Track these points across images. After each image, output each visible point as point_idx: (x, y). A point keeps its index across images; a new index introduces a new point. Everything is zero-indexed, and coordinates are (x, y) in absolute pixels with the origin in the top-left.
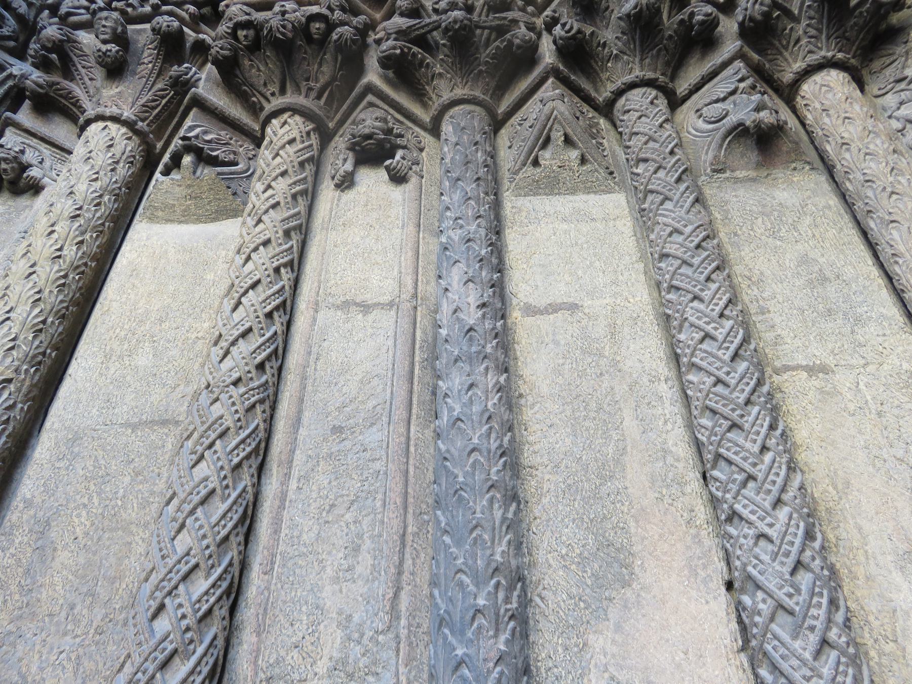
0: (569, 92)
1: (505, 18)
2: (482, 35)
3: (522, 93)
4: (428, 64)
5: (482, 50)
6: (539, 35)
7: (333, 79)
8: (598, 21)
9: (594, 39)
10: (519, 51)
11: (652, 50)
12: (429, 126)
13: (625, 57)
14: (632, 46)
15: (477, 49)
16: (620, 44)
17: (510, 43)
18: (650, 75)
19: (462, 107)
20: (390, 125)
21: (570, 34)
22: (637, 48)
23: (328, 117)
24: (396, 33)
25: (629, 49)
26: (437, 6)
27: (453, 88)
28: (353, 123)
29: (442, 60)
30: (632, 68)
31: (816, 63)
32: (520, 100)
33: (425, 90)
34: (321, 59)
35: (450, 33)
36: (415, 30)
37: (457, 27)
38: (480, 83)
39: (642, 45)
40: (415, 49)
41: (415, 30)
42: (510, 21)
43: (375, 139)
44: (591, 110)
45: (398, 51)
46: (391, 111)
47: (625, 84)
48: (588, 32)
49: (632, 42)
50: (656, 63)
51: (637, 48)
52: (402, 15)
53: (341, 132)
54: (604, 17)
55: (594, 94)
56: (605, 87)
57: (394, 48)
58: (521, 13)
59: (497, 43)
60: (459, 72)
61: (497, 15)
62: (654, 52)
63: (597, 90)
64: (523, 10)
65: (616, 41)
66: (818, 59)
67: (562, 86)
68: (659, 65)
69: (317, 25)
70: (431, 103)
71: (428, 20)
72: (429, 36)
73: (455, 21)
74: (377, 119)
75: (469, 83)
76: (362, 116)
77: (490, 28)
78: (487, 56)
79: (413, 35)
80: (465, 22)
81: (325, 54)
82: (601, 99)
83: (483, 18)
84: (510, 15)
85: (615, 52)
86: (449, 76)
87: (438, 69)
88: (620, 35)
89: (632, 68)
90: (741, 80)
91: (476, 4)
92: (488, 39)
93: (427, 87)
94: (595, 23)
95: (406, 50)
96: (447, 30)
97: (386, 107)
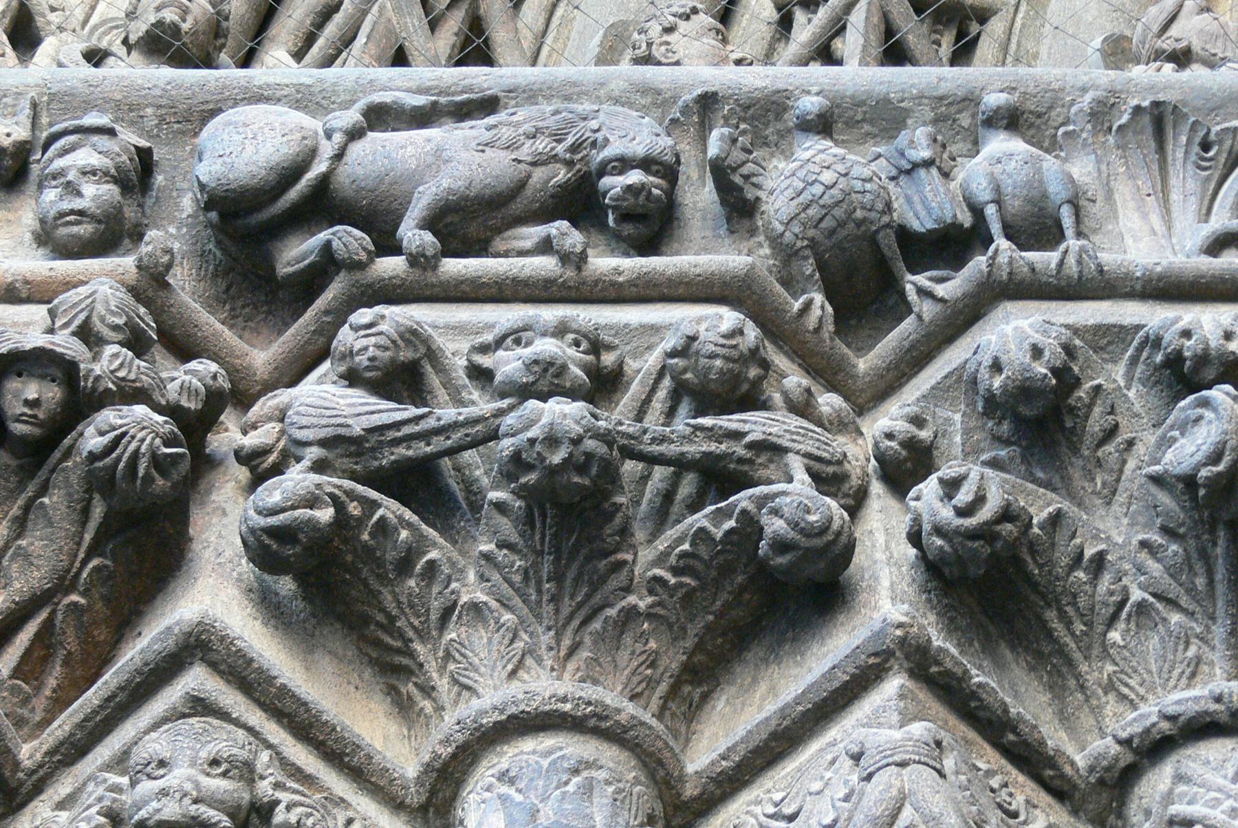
0: (964, 729)
1: (737, 435)
2: (645, 478)
3: (783, 712)
4: (432, 563)
5: (640, 535)
6: (856, 504)
7: (64, 583)
8: (1076, 474)
9: (1061, 537)
10: (782, 560)
12: (415, 797)
13: (1175, 618)
14: (1200, 582)
15: (625, 531)
16: (1155, 567)
17: (750, 527)
19: (548, 741)
20: (264, 788)
22: (1221, 588)
23: (19, 722)
24: (323, 443)
25: (1191, 590)
26: (485, 361)
27: (520, 664)
28: (120, 762)
29: (487, 557)
30: (1198, 660)
32: (774, 736)
33: (411, 654)
34: (27, 509)
35: (531, 478)
36: (396, 442)
37: (557, 458)
38: (623, 656)
40: (390, 508)
41: (396, 442)
42: (752, 446)
44: (1044, 798)
45: (325, 515)
46: (275, 733)
47: (1172, 718)
48: (1039, 515)
49: (1199, 567)
51: (1221, 588)
52: (352, 378)
53: (63, 787)
54: (1099, 463)
55: (1055, 737)
56: (1097, 711)
57: (312, 502)
58: (795, 422)
59: (699, 519)
60: (548, 609)
61: (707, 421)
63: (1065, 718)
64: (803, 408)
65: (1143, 556)
67: (936, 708)
69: (32, 390)
70: (427, 705)
71: (448, 414)
72: (446, 463)
73: (552, 440)
74: (215, 762)
75: (585, 654)
76: (156, 745)
77: (681, 464)
78: (661, 560)
79: (388, 458)
80: (590, 444)
81: (43, 490)
82: (1081, 760)
83: (653, 421)
84: (754, 424)
85: (1136, 595)
86: (507, 617)
87: (471, 590)
88: (1157, 538)
89: (1198, 660)
91: (631, 365)
92: (668, 497)
93: (418, 647)
94: (1067, 480)
95: (354, 509)
96: (518, 463)
97: (256, 717)
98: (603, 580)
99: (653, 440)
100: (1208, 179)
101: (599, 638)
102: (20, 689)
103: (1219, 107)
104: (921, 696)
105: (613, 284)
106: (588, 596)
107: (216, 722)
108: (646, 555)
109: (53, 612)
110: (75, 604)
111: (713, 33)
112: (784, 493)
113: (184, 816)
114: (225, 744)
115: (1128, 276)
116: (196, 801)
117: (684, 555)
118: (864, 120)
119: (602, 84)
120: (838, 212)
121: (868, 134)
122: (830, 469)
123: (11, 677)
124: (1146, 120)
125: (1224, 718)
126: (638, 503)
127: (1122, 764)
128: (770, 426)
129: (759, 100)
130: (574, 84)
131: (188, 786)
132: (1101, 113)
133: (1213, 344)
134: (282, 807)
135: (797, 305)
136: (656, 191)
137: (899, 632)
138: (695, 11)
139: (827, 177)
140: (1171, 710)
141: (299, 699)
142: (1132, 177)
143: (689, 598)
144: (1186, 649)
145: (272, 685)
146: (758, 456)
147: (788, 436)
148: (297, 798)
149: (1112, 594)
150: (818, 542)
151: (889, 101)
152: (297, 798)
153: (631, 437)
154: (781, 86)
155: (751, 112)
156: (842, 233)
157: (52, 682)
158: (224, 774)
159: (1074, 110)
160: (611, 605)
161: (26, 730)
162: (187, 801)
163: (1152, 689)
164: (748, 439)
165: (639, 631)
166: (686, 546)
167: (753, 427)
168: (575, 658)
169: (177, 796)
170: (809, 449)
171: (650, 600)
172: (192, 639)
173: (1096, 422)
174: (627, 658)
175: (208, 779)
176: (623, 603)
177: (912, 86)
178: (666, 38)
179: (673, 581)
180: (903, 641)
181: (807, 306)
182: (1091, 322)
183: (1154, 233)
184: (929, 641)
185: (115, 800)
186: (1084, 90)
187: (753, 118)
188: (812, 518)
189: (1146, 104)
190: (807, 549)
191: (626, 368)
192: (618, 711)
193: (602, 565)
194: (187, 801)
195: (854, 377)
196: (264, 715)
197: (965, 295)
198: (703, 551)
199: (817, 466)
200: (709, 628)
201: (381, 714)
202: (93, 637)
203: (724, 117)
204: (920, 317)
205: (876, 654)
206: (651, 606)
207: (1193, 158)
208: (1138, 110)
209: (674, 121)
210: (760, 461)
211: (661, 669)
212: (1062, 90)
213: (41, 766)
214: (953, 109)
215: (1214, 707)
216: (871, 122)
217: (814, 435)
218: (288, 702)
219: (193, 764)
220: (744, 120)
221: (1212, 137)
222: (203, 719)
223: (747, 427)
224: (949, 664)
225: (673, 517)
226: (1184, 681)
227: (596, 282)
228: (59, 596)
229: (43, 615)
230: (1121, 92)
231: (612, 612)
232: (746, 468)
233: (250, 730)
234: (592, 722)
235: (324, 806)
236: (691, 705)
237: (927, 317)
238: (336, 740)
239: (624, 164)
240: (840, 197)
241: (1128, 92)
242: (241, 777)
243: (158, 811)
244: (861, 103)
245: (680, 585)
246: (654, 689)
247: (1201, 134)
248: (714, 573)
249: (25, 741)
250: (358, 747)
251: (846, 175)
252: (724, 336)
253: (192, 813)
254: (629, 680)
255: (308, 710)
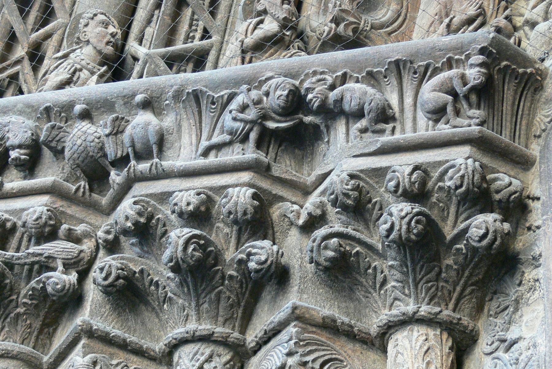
1: (41, 255)
11: (210, 292)
13: (181, 301)
14: (186, 289)
17: (44, 289)
18: (205, 327)
21: (106, 283)
22: (192, 291)
25: (183, 292)
30: (188, 315)
31: (396, 319)
38: (19, 327)
39: (196, 290)
42: (46, 257)
47: (175, 339)
50: (218, 308)
51: (192, 291)
55: (146, 344)
62: (213, 296)
66: (397, 316)
68: (221, 310)
75: (7, 329)
78: (25, 296)
89: (188, 315)
90: (290, 354)
98: (8, 306)
99: (16, 259)
100: (214, 116)
101: (10, 323)
103: (219, 86)
104: (92, 344)
105: (13, 193)
106: (4, 312)
108: (23, 292)
111: (101, 25)
112: (51, 277)
115: (173, 171)
117: (30, 295)
118: (101, 107)
119: (15, 106)
120: (83, 155)
121: (103, 112)
122: (72, 261)
124: (192, 96)
125: (190, 338)
126: (22, 273)
127: (166, 351)
128: (51, 250)
129: (65, 105)
130: (6, 107)
132: (177, 96)
133: (183, 208)
135: (74, 188)
136: (23, 157)
137: (80, 328)
138: (95, 15)
139: (79, 142)
140: (175, 336)
142: (189, 119)
143: (36, 306)
144: (184, 311)
146: (49, 260)
147: (56, 253)
149: (162, 294)
150: (61, 294)
151: (107, 100)
153: (9, 259)
154: (72, 99)
155: (64, 109)
156: (86, 161)
159: (168, 96)
160: (12, 313)
163: (176, 324)
164: (44, 256)
165: (22, 319)
166: (31, 292)
167: (46, 251)
168: (3, 331)
170: (64, 257)
171: (24, 309)
173: (160, 230)
174: (21, 327)
176: (15, 312)
177: (115, 93)
178: (85, 29)
179: (30, 302)
180: (82, 330)
181: (78, 189)
182: (160, 191)
183: (191, 144)
184: (91, 327)
186: (172, 86)
187: (65, 111)
188: (59, 286)
189: (190, 91)
190: (59, 296)
191: (17, 224)
192: (13, 351)
193: (6, 301)
195: (102, 206)
197: (123, 183)
198: (36, 293)
199: (67, 261)
200: (47, 313)
203: (54, 114)
204: (114, 189)
205: (77, 333)
206: (26, 310)
207: (209, 109)
208: (188, 93)
209: (38, 118)
210: (50, 261)
211: (34, 328)
212: (164, 87)
214: (130, 99)
215: (186, 335)
216: (103, 107)
217: (67, 250)
220: (63, 112)
221: (215, 100)
223: (44, 251)
224: (100, 333)
225: (33, 276)
226: (184, 322)
227: (7, 193)
230: (185, 85)
231: (12, 315)
232: (46, 264)
234: (6, 355)
236: (49, 334)
237: (115, 188)
239: (14, 148)
240: (83, 150)
241: (187, 85)
244: (99, 102)
245: (32, 304)
246: (32, 334)
247: (211, 99)
248: (42, 298)
251: (85, 140)
252: (34, 221)
254: (22, 335)
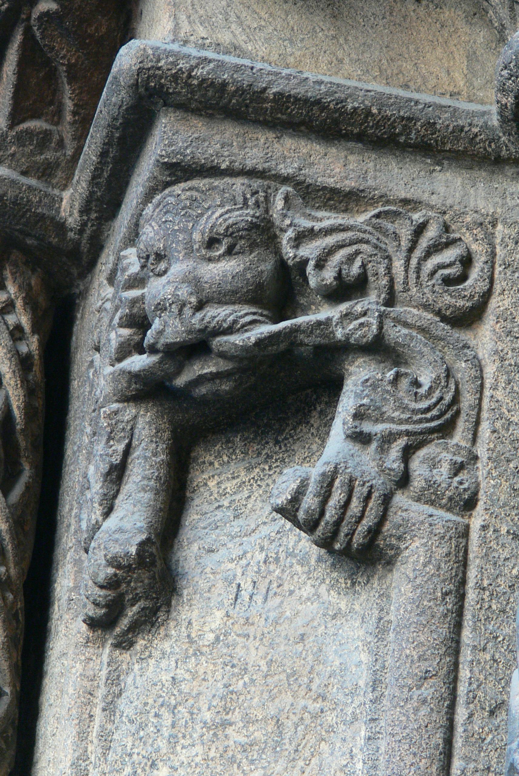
43: (223, 355)
102: (29, 133)
107: (201, 183)
109: (28, 32)
110: (47, 14)
113: (189, 332)
114: (220, 211)
116: (200, 306)
123: (11, 127)
131: (184, 292)
134: (310, 269)
141: (306, 101)
145: (265, 100)
148: (330, 240)
152: (330, 240)
157: (69, 105)
158: (230, 252)
161: (59, 174)
162: (188, 312)
169: (175, 309)
172: (142, 90)
175: (211, 266)
185: (134, 302)
194: (188, 312)
196: (271, 135)
201: (460, 24)
202: (91, 36)
213: (84, 225)
218: (294, 110)
219: (189, 251)
222: (189, 184)
228: (25, 9)
229: (18, 38)
233: (252, 173)
235: (378, 228)
238: (377, 125)
242: (253, 246)
243: (161, 333)
249: (64, 187)
250: (409, 119)
253: (197, 326)
255: (324, 108)
